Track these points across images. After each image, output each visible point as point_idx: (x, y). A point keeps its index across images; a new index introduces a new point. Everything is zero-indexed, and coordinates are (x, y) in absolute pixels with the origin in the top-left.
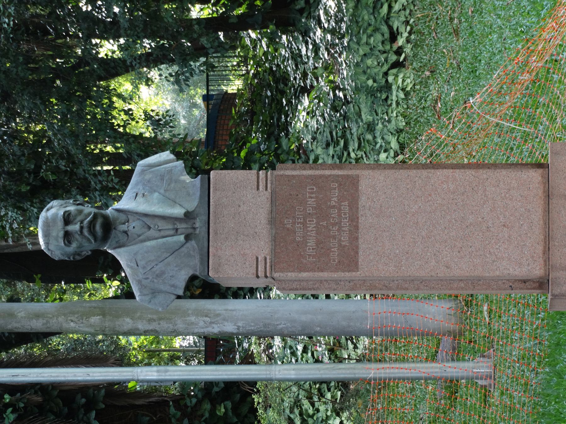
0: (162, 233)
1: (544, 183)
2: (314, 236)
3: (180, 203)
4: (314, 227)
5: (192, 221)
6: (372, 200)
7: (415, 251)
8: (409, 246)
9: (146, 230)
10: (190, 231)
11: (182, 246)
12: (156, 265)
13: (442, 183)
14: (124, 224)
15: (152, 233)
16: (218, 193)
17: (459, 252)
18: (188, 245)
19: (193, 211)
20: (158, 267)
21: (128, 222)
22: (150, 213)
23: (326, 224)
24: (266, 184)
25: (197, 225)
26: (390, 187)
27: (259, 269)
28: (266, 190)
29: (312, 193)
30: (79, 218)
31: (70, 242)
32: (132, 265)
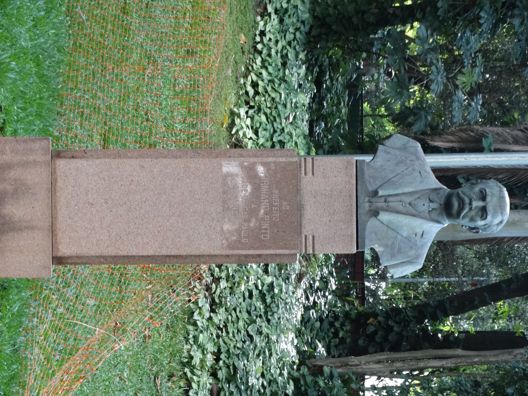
0: (398, 198)
1: (56, 243)
2: (263, 194)
3: (383, 225)
4: (262, 202)
5: (372, 208)
6: (211, 227)
7: (172, 181)
8: (177, 186)
9: (413, 202)
10: (374, 200)
11: (380, 186)
12: (403, 171)
13: (148, 243)
14: (433, 209)
15: (408, 200)
16: (349, 233)
17: (132, 180)
18: (375, 187)
19: (371, 217)
20: (401, 170)
21: (429, 211)
22: (410, 217)
23: (251, 206)
24: (306, 242)
25: (367, 205)
26: (195, 239)
27: (311, 165)
28: (306, 236)
29: (265, 233)
30: (473, 213)
31: (481, 192)
32: (425, 174)
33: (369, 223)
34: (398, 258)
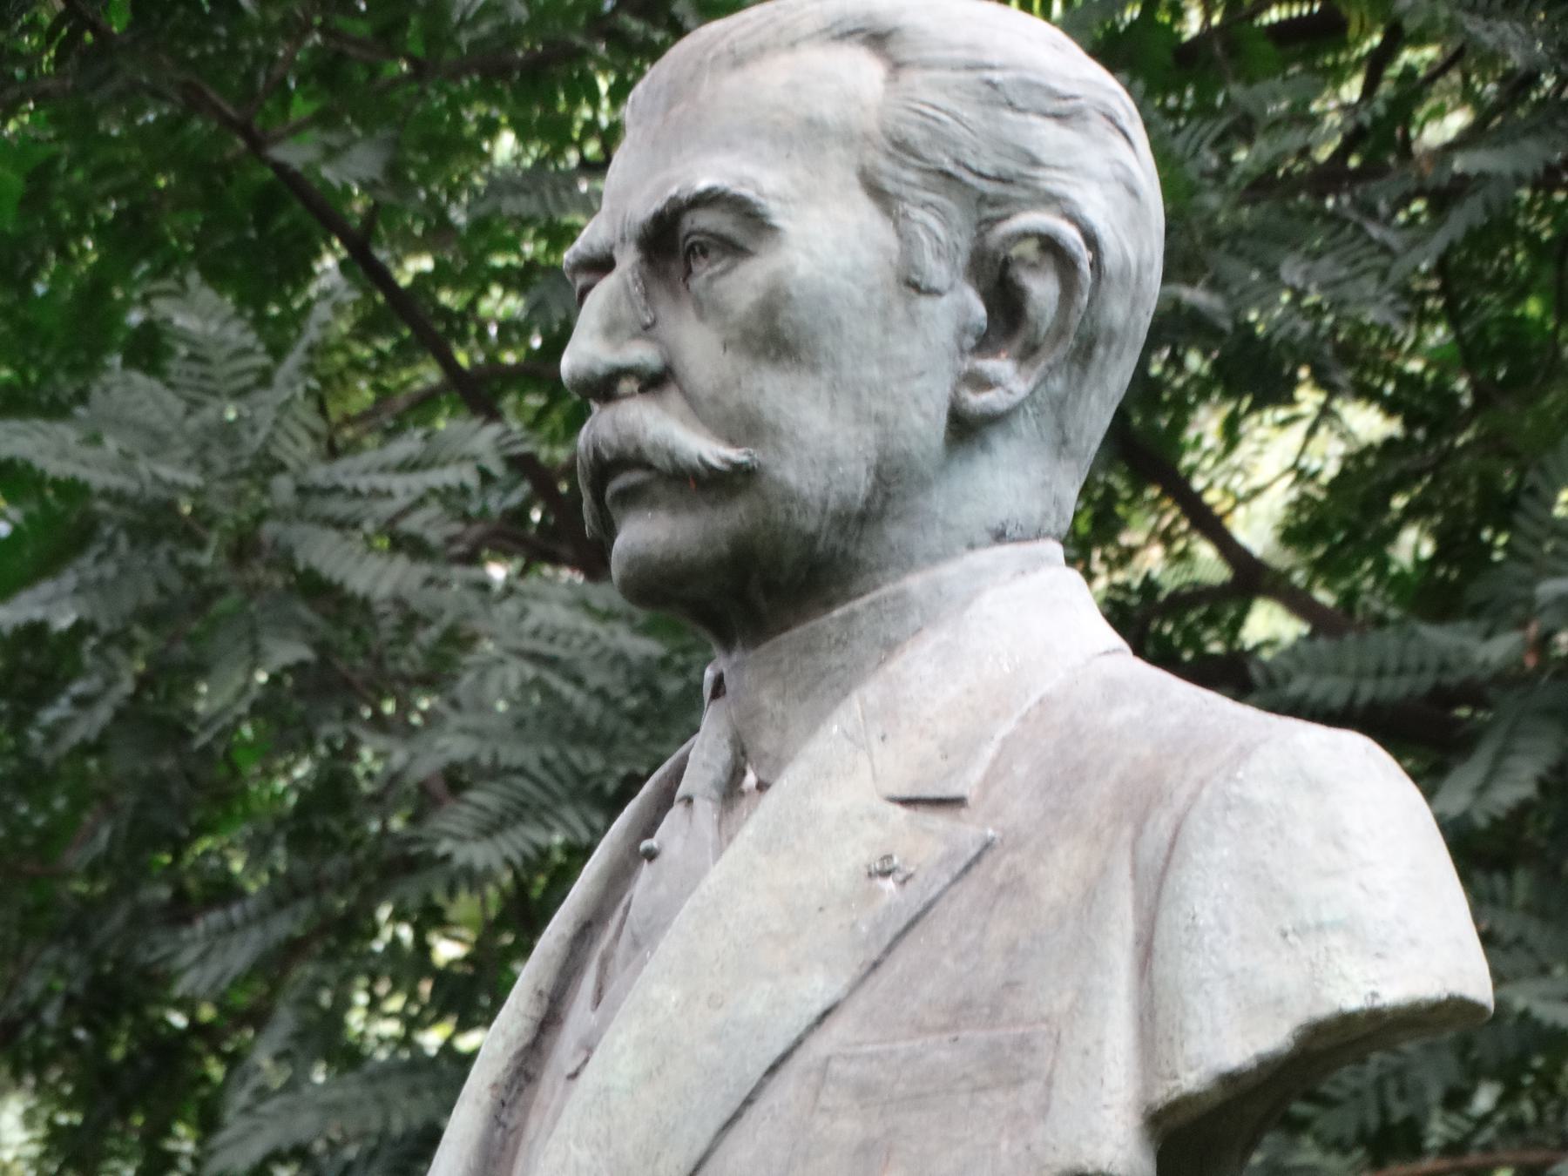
30: (699, 348)
34: (1061, 1004)
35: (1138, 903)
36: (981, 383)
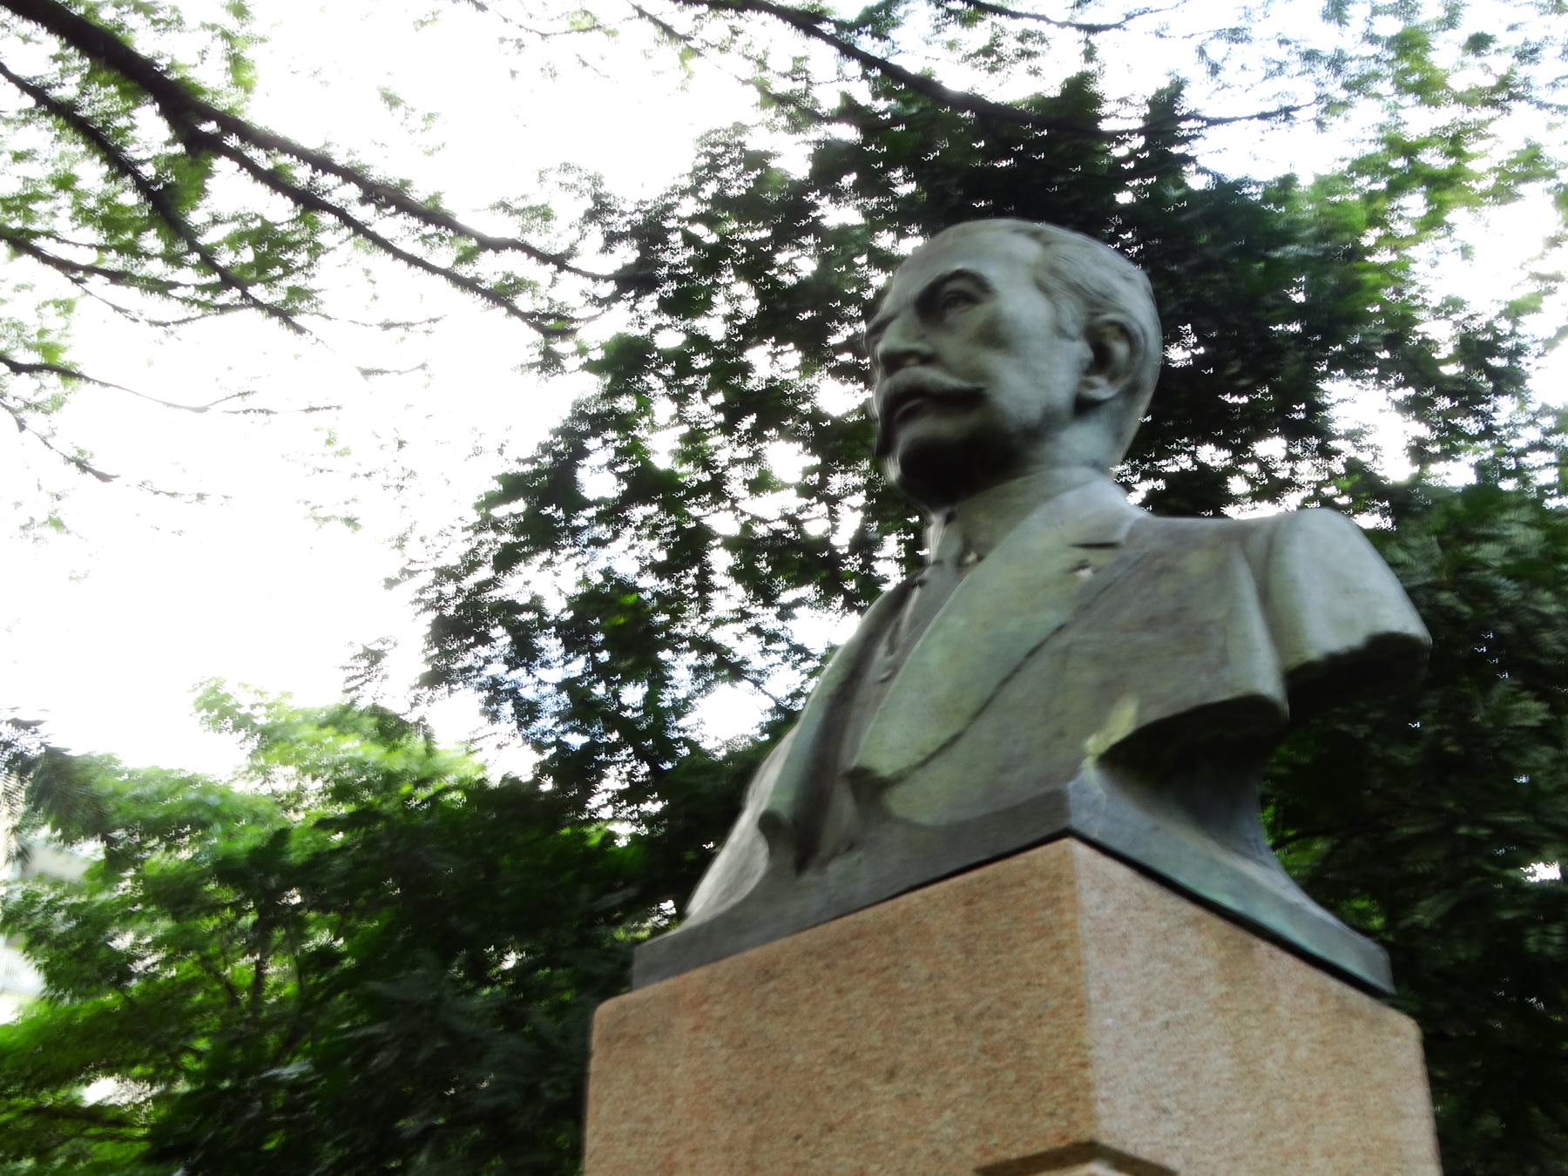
19: (887, 817)
33: (925, 819)
34: (1219, 614)
35: (1254, 574)
36: (1092, 386)
